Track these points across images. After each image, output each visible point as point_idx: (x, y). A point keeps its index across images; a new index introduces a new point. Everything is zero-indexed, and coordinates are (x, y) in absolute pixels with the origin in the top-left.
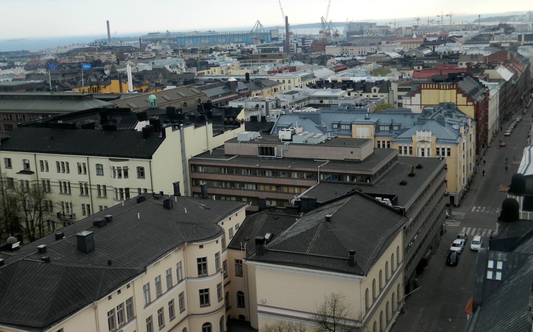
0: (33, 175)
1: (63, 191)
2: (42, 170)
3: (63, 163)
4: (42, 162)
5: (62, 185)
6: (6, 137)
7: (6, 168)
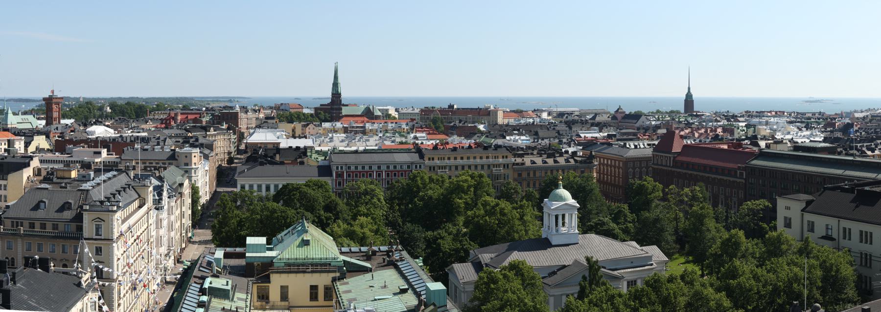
0: (834, 241)
1: (864, 264)
2: (845, 238)
3: (866, 232)
4: (845, 229)
5: (863, 256)
6: (811, 199)
7: (808, 231)
